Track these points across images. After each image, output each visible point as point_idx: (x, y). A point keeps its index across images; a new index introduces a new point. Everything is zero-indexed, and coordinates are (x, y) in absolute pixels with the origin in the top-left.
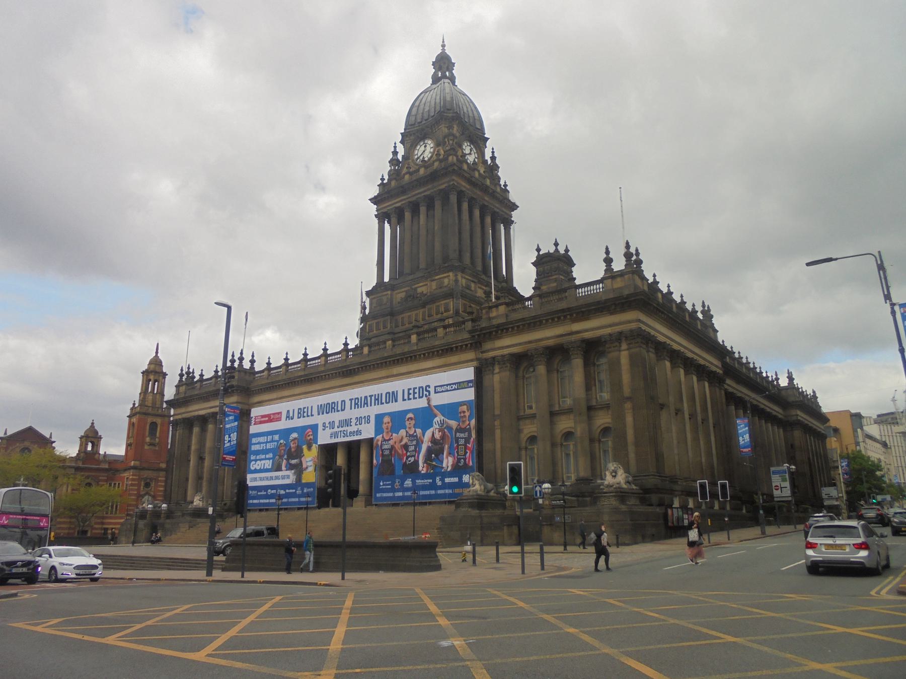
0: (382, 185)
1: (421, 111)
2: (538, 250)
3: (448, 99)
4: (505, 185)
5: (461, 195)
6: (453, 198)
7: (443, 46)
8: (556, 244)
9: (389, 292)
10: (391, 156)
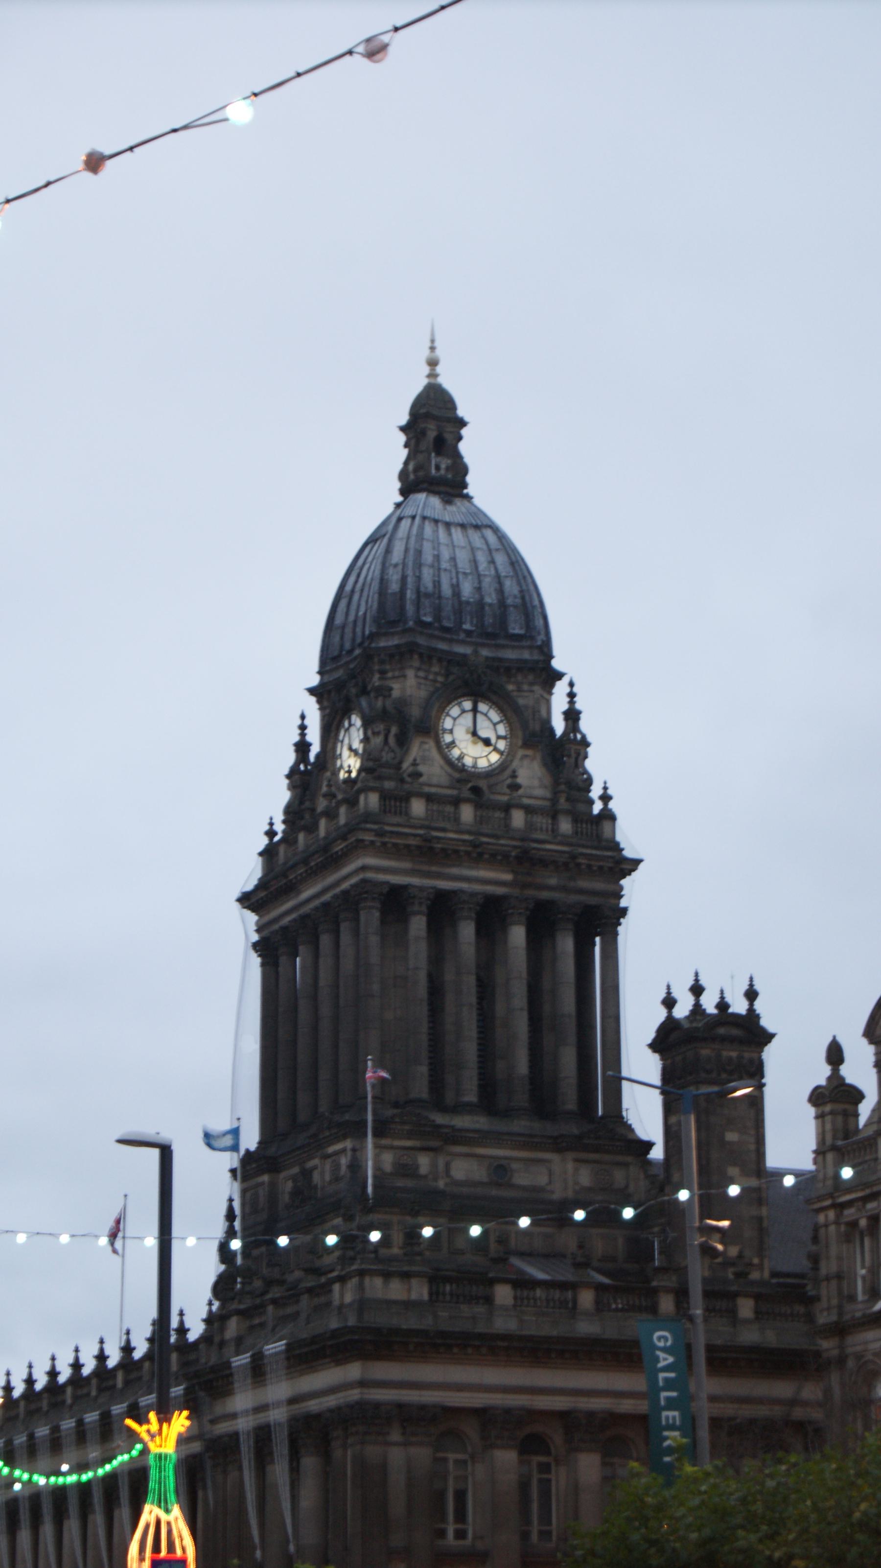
0: (268, 853)
1: (351, 618)
2: (669, 1002)
3: (394, 587)
4: (606, 798)
5: (395, 902)
6: (370, 917)
7: (433, 363)
8: (697, 990)
9: (265, 1178)
10: (290, 758)
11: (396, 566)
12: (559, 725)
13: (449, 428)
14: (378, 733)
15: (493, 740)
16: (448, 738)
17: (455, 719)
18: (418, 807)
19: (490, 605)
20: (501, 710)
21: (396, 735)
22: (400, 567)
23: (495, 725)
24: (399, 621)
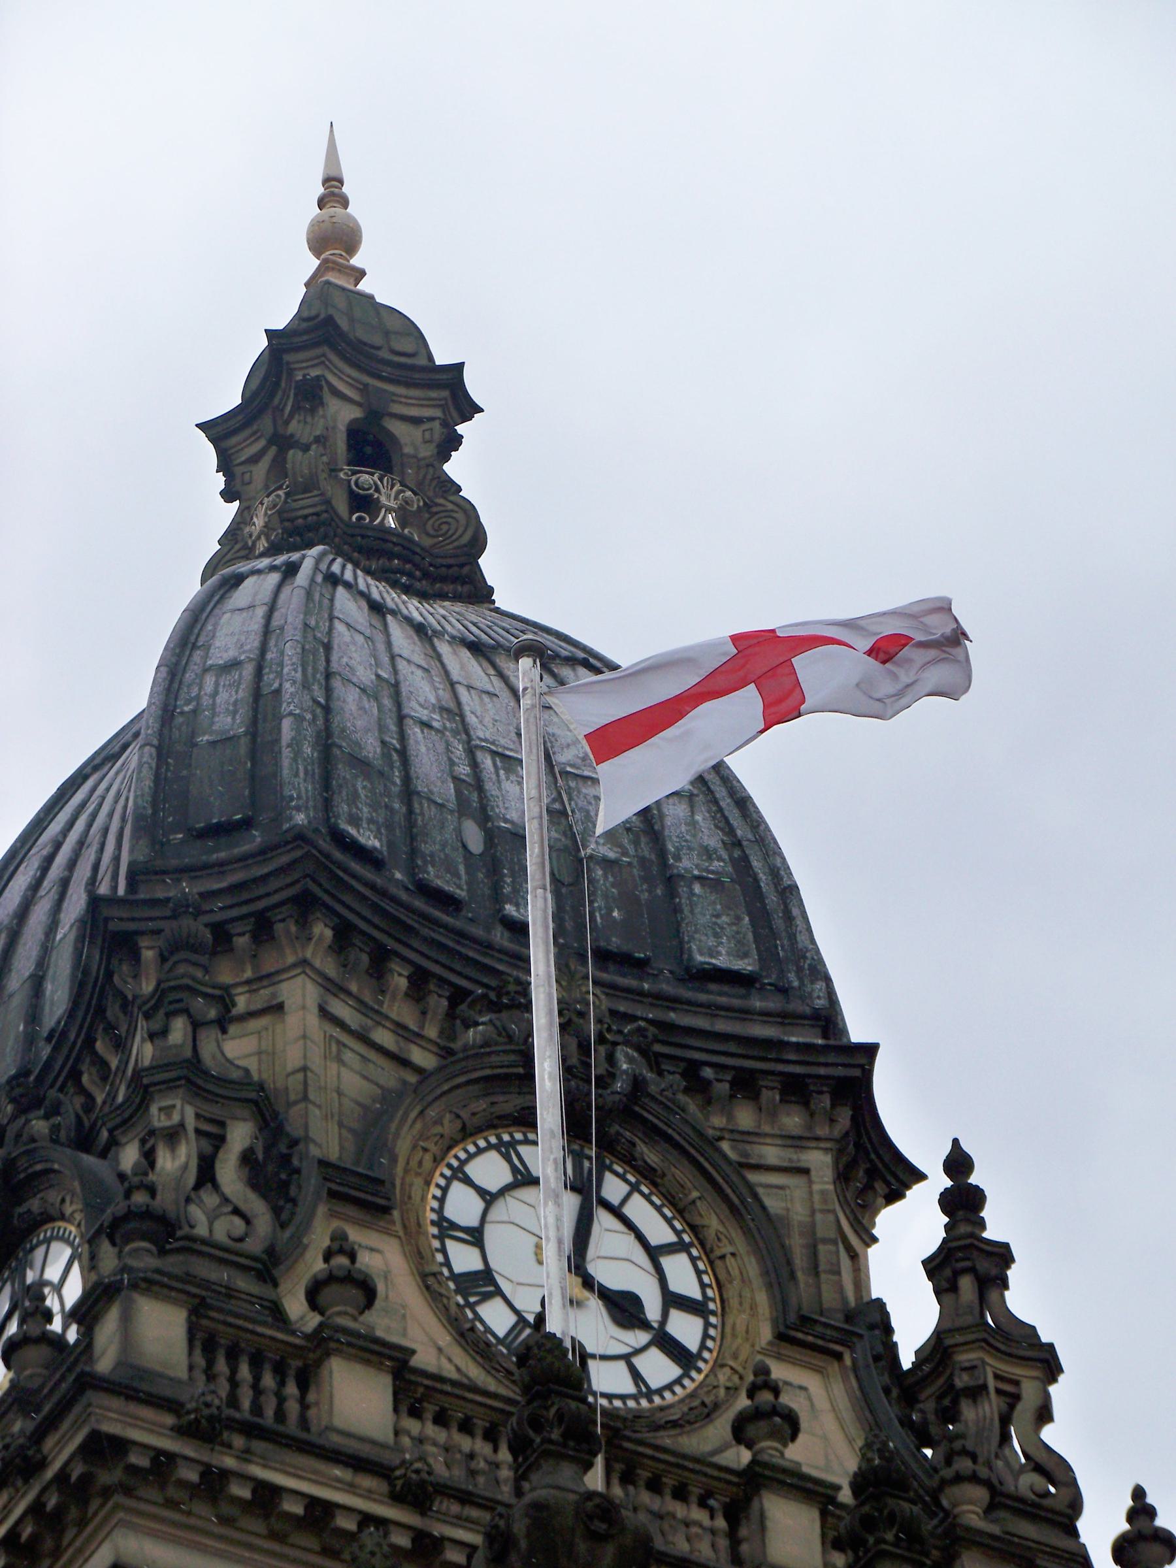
11: (234, 664)
12: (915, 1320)
13: (407, 402)
14: (173, 1136)
15: (653, 1311)
16: (464, 1259)
17: (489, 1198)
18: (357, 1401)
19: (607, 863)
20: (675, 1205)
21: (247, 1158)
22: (248, 670)
23: (654, 1253)
24: (247, 824)
